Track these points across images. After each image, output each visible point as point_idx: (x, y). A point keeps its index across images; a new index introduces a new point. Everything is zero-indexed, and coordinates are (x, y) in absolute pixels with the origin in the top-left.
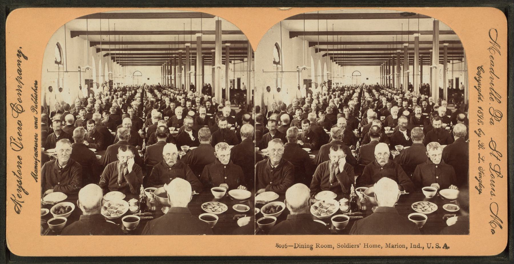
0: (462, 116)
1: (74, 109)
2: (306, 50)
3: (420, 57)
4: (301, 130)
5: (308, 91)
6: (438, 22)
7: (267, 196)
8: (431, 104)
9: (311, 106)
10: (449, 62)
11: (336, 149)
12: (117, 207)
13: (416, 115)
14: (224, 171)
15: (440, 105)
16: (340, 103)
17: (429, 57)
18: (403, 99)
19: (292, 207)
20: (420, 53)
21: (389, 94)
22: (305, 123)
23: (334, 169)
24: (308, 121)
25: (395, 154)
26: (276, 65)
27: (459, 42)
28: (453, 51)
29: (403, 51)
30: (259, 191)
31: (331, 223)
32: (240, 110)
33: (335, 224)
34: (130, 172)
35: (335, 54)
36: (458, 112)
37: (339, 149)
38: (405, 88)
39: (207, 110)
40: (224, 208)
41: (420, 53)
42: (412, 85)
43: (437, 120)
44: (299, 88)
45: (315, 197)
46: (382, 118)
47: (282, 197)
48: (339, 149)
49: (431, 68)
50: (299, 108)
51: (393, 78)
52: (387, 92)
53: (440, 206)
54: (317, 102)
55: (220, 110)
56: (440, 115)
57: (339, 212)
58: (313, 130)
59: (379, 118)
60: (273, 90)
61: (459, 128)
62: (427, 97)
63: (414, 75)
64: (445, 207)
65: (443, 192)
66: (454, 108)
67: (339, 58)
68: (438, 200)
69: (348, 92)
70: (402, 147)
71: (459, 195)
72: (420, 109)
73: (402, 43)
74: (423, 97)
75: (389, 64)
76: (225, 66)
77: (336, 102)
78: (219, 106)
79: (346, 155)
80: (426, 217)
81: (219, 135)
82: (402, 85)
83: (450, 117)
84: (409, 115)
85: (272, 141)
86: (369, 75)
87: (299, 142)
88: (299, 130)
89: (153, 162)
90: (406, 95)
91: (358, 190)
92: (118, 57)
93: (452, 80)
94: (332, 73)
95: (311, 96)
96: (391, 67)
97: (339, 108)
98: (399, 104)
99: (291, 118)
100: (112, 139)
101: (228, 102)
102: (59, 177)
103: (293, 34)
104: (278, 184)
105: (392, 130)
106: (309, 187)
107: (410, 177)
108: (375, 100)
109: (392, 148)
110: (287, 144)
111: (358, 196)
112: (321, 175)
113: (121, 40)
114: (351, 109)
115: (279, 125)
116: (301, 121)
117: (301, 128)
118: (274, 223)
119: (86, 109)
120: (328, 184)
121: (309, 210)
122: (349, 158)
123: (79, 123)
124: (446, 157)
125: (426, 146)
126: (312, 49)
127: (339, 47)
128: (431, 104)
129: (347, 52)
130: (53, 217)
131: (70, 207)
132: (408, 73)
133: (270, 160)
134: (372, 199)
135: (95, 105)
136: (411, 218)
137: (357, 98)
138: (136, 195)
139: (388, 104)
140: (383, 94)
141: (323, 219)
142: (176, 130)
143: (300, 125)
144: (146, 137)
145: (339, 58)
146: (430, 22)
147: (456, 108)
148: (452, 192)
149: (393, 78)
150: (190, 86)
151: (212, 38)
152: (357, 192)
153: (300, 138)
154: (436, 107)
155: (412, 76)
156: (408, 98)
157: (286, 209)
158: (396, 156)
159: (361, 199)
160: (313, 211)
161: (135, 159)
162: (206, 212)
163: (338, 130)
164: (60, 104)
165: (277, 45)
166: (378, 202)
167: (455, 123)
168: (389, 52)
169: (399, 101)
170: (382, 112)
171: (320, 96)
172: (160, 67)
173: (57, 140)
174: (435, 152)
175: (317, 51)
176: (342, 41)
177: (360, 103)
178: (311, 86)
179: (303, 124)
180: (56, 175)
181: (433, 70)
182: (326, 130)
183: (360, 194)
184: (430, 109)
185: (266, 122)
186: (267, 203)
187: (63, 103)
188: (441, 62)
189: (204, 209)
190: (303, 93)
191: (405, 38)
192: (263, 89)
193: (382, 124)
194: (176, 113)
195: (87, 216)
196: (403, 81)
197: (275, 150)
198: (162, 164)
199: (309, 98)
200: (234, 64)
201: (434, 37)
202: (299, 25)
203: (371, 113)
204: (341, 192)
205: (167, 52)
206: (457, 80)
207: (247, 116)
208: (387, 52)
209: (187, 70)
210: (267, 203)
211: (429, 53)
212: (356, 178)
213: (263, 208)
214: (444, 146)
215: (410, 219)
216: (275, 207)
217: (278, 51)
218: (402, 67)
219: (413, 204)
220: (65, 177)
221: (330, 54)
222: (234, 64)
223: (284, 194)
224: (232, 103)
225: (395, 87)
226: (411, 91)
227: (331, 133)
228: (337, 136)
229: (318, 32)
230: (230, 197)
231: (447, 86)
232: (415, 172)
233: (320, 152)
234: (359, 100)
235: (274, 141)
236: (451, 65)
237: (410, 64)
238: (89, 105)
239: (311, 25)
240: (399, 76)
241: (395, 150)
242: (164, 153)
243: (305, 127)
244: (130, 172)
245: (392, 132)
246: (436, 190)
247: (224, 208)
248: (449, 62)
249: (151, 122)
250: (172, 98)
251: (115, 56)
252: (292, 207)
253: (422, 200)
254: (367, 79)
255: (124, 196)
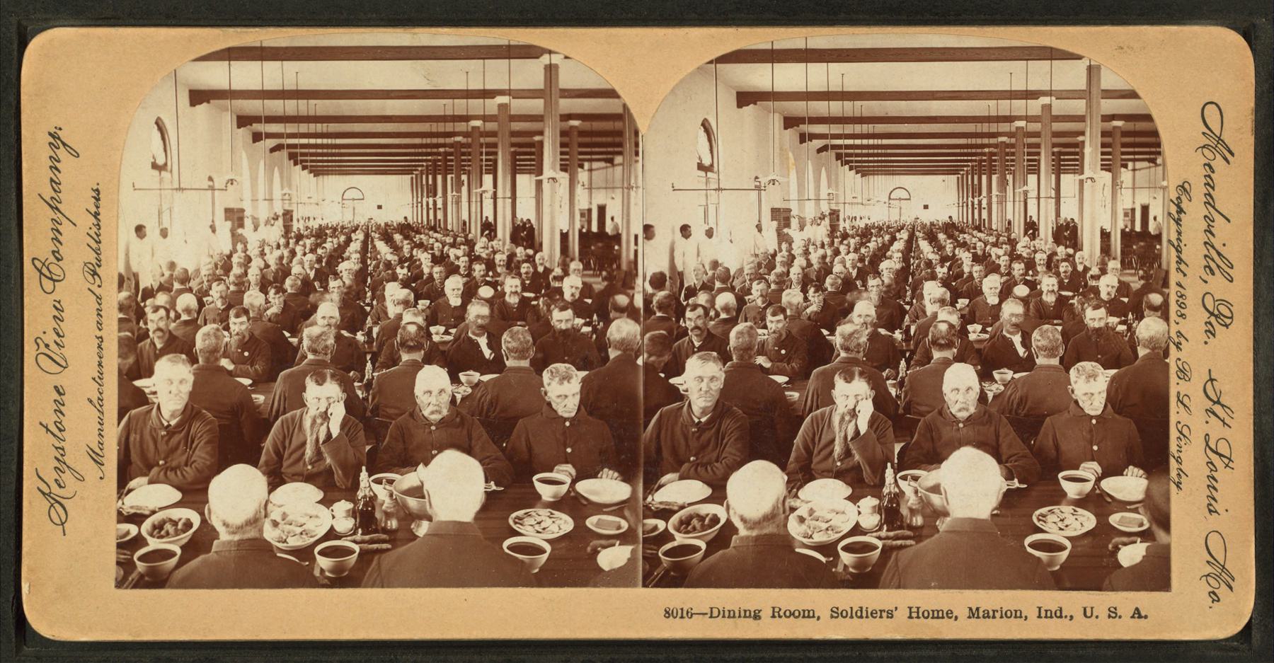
0: (1156, 299)
1: (740, 279)
2: (777, 136)
3: (1053, 154)
4: (765, 331)
5: (782, 238)
6: (1099, 67)
7: (680, 491)
8: (1080, 268)
9: (788, 272)
10: (1126, 166)
11: (849, 379)
12: (829, 516)
13: (1044, 297)
14: (1091, 431)
15: (1103, 271)
16: (859, 265)
17: (1077, 154)
18: (1014, 257)
19: (743, 520)
20: (1054, 145)
21: (980, 244)
22: (774, 314)
23: (844, 427)
24: (783, 310)
25: (993, 390)
26: (703, 174)
27: (1148, 118)
28: (1136, 141)
29: (1013, 140)
30: (664, 479)
31: (837, 556)
32: (1142, 282)
33: (847, 558)
34: (863, 431)
35: (847, 147)
36: (1147, 289)
37: (857, 377)
38: (1018, 230)
39: (1061, 284)
40: (1087, 521)
41: (1054, 145)
42: (1034, 223)
43: (1096, 308)
44: (760, 230)
45: (800, 494)
46: (962, 302)
47: (718, 495)
48: (857, 377)
49: (1081, 182)
50: (760, 278)
51: (989, 204)
52: (974, 240)
53: (1102, 516)
54: (804, 263)
55: (1092, 283)
56: (1104, 296)
57: (857, 530)
58: (794, 331)
59: (953, 303)
60: (698, 232)
61: (1149, 327)
62: (1071, 251)
63: (1039, 198)
64: (1114, 519)
65: (1109, 485)
66: (1136, 278)
67: (857, 155)
68: (1097, 502)
69: (880, 240)
70: (1009, 374)
71: (1148, 491)
72: (1054, 281)
73: (1009, 119)
74: (1061, 250)
75: (979, 170)
76: (1107, 176)
77: (848, 264)
78: (1091, 273)
79: (873, 393)
80: (1068, 544)
81: (1080, 346)
82: (1009, 223)
83: (1126, 300)
84: (1028, 296)
85: (695, 356)
86: (933, 198)
87: (761, 360)
88: (760, 331)
89: (923, 409)
90: (1019, 246)
91: (904, 478)
92: (851, 155)
93: (1133, 210)
94: (841, 193)
95: (790, 250)
96: (984, 178)
97: (857, 278)
98: (1003, 269)
99: (741, 301)
100: (822, 352)
101: (1114, 265)
102: (694, 444)
103: (745, 98)
104: (710, 463)
105: (986, 332)
106: (783, 467)
107: (1030, 447)
108: (943, 260)
109: (985, 376)
110: (732, 366)
111: (902, 493)
112: (813, 440)
113: (857, 114)
114: (887, 281)
115: (711, 319)
116: (765, 308)
117: (765, 327)
118: (699, 555)
119: (772, 277)
120: (830, 460)
121: (785, 526)
122: (882, 401)
123: (751, 315)
124: (1115, 398)
125: (1067, 370)
126: (791, 134)
127: (858, 128)
128: (1080, 268)
129: (876, 142)
130: (147, 544)
131: (715, 516)
132: (1026, 193)
133: (690, 405)
134: (936, 499)
135: (793, 270)
136: (1031, 545)
137: (900, 255)
138: (876, 488)
139: (977, 268)
140: (964, 245)
141: (820, 548)
142: (984, 331)
143: (763, 319)
144: (375, 349)
145: (857, 155)
146: (1081, 66)
147: (1141, 278)
148: (1130, 485)
149: (989, 204)
150: (1026, 223)
151: (1078, 106)
152: (900, 482)
153: (762, 351)
154: (1096, 278)
155: (1035, 201)
156: (1024, 255)
157: (729, 522)
158: (995, 397)
159: (911, 500)
160: (794, 529)
161: (875, 401)
162: (1042, 531)
163: (855, 332)
164: (707, 267)
165: (705, 125)
166: (951, 508)
167: (1140, 317)
168: (979, 141)
169: (1003, 262)
170: (959, 287)
171: (811, 249)
172: (954, 178)
173: (157, 357)
174: (1091, 387)
175: (803, 138)
176: (865, 114)
177: (908, 265)
178: (788, 225)
179: (769, 318)
180: (686, 439)
181: (1087, 185)
182: (825, 332)
183: (908, 488)
184: (1078, 282)
185: (680, 312)
186: (682, 507)
187: (715, 264)
188: (1106, 167)
189: (1038, 524)
190: (769, 241)
191: (1018, 106)
192: (673, 232)
193: (962, 316)
194: (985, 289)
195: (747, 537)
196: (1013, 212)
197: (701, 379)
198: (940, 413)
199: (785, 253)
200: (1134, 170)
201: (1089, 106)
202: (759, 77)
203: (932, 290)
204: (861, 481)
205: (969, 141)
206: (1145, 209)
207: (1156, 299)
208: (973, 141)
209: (1017, 185)
210: (682, 507)
211: (1076, 145)
212: (897, 448)
213: (674, 519)
214: (1113, 372)
215: (1030, 550)
216: (701, 518)
217: (710, 140)
218: (1009, 177)
219: (1038, 512)
220: (177, 448)
221: (834, 147)
222: (1134, 170)
223: (724, 487)
224: (1125, 264)
225: (994, 227)
226: (1033, 237)
227: (837, 340)
228: (852, 346)
229: (843, 92)
230: (1104, 494)
231: (1121, 225)
232: (1040, 437)
233: (812, 383)
234: (906, 258)
235: (700, 357)
236: (1131, 173)
237: (1031, 172)
238: (779, 269)
239: (789, 77)
240: (1002, 201)
241: (993, 380)
242: (946, 388)
243: (775, 322)
244: (863, 431)
245: (987, 336)
246: (1093, 478)
247: (1087, 521)
248: (1126, 166)
249: (924, 312)
250: (980, 253)
251: (843, 151)
252: (743, 520)
253: (1058, 503)
254: (926, 207)
255: (849, 491)
